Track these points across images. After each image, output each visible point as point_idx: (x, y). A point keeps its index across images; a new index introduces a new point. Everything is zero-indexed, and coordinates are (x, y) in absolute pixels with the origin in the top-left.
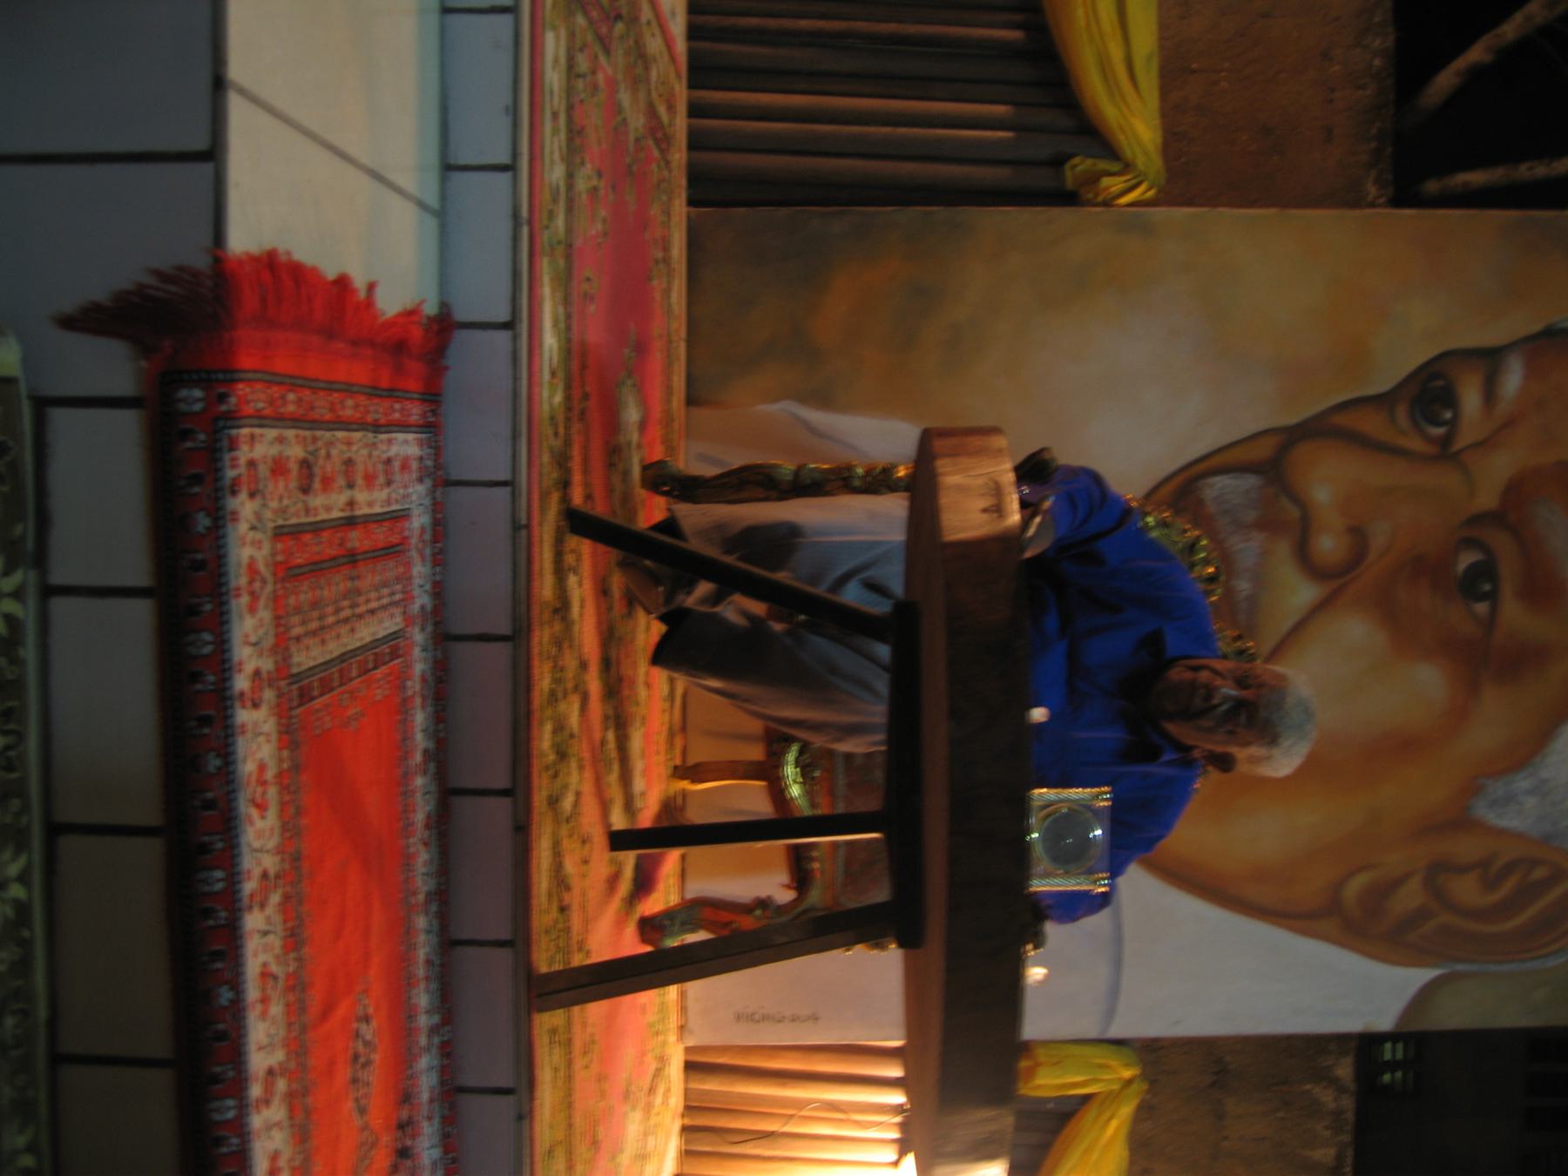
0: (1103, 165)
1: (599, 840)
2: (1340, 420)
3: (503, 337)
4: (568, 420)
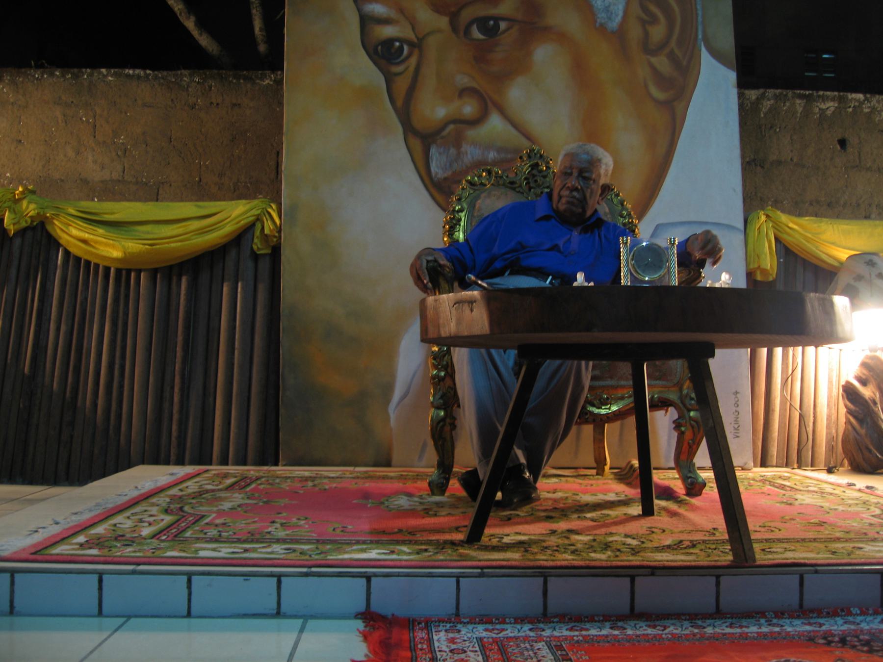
0: (258, 233)
1: (647, 522)
2: (399, 103)
3: (374, 580)
4: (416, 543)
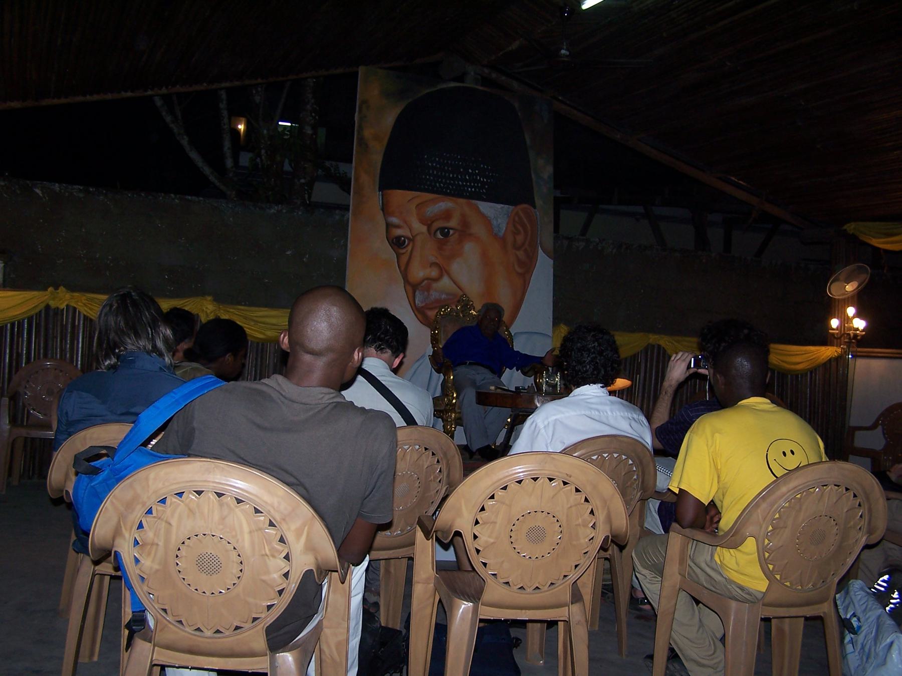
2: (402, 269)
